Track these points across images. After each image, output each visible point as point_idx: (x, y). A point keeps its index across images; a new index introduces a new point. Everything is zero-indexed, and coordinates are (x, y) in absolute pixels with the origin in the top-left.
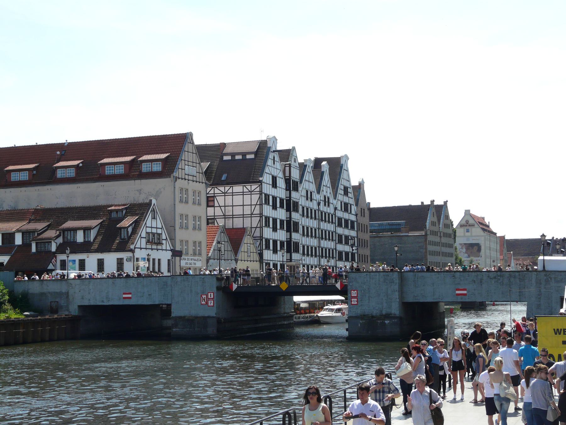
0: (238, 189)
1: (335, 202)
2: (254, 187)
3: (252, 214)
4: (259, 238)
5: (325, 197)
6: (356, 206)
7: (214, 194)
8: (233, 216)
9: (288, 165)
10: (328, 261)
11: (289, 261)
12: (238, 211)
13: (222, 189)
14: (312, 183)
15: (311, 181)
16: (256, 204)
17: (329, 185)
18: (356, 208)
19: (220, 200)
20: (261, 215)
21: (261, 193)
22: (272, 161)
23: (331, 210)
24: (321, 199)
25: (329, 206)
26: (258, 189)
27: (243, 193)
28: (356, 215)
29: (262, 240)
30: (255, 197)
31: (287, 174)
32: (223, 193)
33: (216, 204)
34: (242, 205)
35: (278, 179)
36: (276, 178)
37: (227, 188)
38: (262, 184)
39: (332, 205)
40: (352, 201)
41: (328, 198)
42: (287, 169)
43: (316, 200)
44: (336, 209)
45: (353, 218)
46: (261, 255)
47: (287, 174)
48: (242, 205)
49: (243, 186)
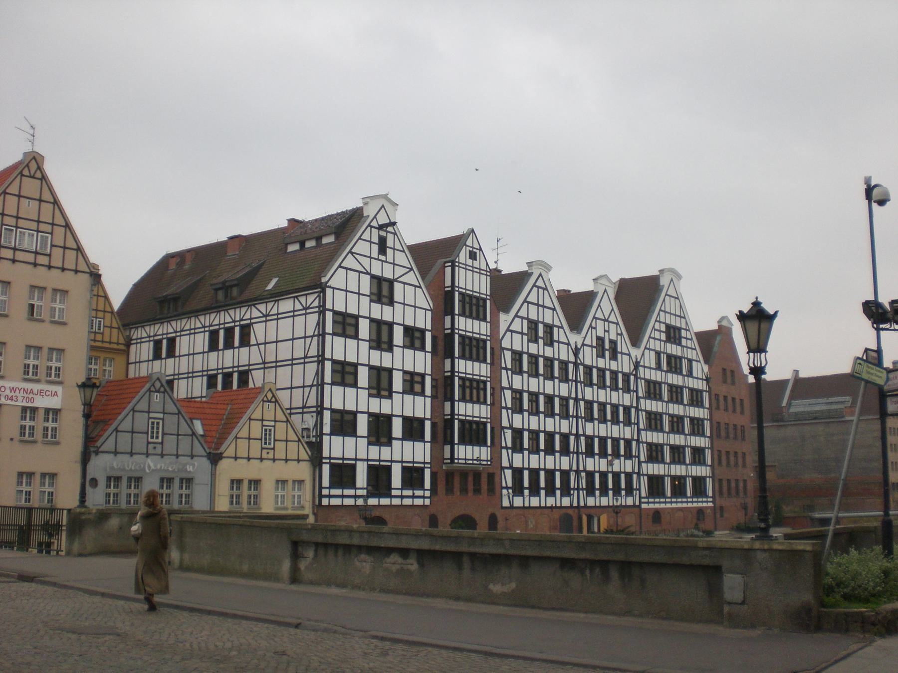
0: (286, 305)
1: (635, 353)
2: (311, 298)
3: (306, 357)
4: (314, 409)
5: (600, 340)
6: (706, 362)
7: (251, 319)
8: (277, 364)
9: (450, 264)
10: (610, 464)
11: (449, 461)
12: (284, 351)
13: (262, 307)
14: (554, 309)
15: (548, 303)
16: (313, 336)
17: (616, 317)
18: (706, 368)
19: (258, 332)
20: (320, 358)
21: (322, 310)
22: (375, 248)
23: (624, 365)
24: (587, 341)
25: (614, 357)
26: (316, 303)
27: (293, 314)
28: (707, 380)
29: (320, 414)
30: (313, 319)
31: (448, 282)
32: (264, 316)
33: (253, 341)
34: (290, 340)
35: (398, 287)
36: (391, 283)
37: (270, 305)
38: (324, 291)
39: (626, 358)
40: (694, 354)
41: (613, 343)
42: (448, 271)
43: (568, 344)
44: (637, 365)
45: (701, 385)
46: (316, 448)
47: (448, 282)
48: (290, 340)
49: (294, 297)
